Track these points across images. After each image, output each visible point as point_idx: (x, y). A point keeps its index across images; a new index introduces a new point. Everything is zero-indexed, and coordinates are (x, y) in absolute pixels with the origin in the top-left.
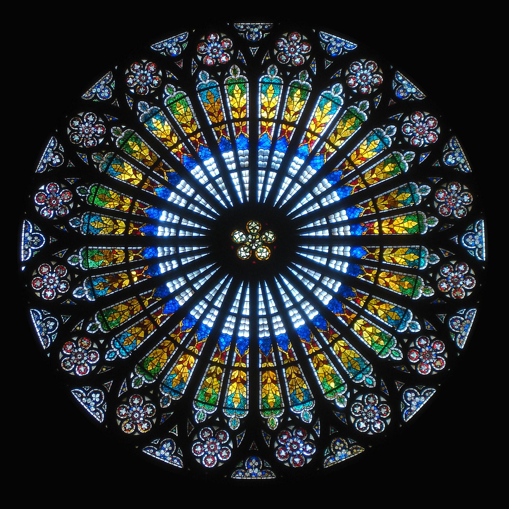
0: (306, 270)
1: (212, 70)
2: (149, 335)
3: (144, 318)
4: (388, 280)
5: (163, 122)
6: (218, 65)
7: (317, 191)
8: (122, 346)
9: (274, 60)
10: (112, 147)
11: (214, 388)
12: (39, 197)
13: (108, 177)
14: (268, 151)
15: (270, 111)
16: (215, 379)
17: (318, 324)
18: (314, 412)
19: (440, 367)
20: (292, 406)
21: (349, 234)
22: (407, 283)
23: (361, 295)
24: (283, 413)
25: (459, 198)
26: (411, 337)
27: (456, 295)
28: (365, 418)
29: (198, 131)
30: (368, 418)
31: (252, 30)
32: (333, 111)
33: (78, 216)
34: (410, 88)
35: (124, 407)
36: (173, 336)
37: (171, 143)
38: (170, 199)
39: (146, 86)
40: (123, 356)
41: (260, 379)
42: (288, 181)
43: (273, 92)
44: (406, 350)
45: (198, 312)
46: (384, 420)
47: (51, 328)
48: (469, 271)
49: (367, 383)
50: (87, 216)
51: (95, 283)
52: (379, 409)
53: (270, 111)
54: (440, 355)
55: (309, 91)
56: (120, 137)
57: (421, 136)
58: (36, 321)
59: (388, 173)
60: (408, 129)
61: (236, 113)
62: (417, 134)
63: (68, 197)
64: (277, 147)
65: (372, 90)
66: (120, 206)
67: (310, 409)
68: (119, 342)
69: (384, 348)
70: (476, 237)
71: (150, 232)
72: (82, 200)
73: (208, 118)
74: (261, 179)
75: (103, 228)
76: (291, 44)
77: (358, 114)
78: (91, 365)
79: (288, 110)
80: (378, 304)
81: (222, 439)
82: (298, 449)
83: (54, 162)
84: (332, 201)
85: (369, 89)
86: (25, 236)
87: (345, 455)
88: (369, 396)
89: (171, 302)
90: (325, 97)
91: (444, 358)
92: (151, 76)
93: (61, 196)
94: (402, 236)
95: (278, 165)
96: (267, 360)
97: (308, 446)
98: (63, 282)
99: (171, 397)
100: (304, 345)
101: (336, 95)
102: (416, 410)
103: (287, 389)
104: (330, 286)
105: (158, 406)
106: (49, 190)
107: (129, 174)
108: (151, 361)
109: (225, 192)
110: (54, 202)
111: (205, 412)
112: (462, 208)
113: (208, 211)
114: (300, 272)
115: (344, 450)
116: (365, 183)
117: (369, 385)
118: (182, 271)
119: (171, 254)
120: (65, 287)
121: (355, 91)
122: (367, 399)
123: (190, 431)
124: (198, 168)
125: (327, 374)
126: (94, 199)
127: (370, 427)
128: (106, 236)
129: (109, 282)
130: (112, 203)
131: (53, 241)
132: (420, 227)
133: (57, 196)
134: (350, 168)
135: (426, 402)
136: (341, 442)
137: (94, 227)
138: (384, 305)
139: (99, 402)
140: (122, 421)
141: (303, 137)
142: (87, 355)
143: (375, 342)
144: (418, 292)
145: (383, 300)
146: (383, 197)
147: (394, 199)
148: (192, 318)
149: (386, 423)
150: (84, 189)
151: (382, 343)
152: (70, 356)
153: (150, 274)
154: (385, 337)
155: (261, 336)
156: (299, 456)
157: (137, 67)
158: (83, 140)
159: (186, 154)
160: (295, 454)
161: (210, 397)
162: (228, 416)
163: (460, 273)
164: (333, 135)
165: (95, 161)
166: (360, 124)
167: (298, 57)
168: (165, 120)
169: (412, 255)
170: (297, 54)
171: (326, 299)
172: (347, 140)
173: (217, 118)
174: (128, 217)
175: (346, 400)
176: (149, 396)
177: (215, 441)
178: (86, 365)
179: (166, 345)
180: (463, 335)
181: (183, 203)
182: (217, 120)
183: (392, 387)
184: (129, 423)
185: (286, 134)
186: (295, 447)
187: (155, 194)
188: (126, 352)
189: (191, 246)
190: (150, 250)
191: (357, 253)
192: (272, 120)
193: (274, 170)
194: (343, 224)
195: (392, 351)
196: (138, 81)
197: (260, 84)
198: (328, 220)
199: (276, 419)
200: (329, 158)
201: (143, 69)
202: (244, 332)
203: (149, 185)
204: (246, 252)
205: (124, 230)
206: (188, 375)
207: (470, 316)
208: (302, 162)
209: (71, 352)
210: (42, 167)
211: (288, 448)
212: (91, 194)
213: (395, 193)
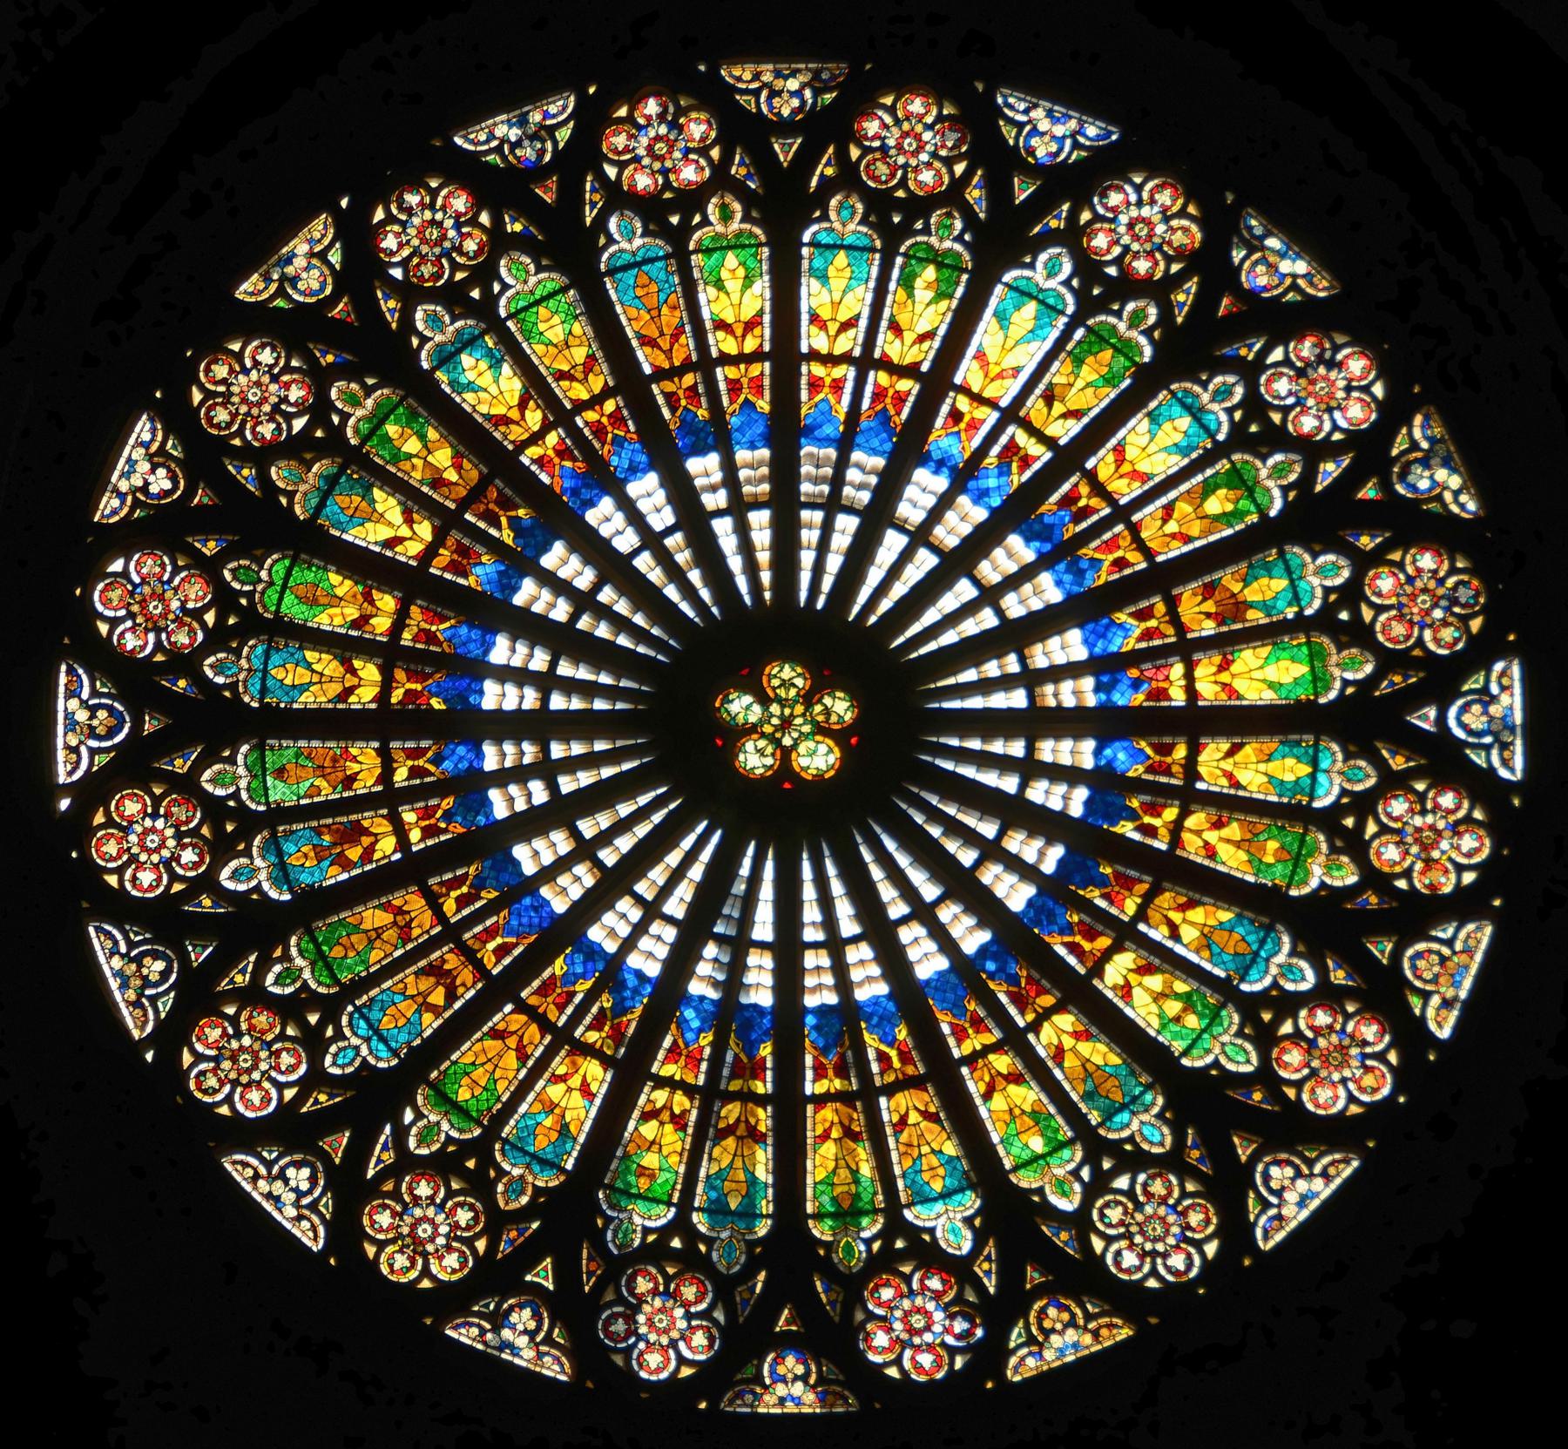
1: (650, 209)
2: (457, 998)
3: (445, 949)
4: (1212, 836)
5: (496, 365)
6: (668, 195)
7: (991, 570)
8: (377, 1032)
9: (848, 178)
10: (335, 444)
11: (665, 1152)
12: (110, 594)
13: (322, 532)
14: (832, 453)
16: (669, 1128)
17: (991, 966)
18: (977, 1222)
19: (1375, 1090)
20: (909, 1205)
21: (1091, 701)
23: (1128, 884)
26: (1287, 1004)
27: (1427, 882)
28: (1138, 1239)
29: (607, 393)
30: (1147, 1239)
31: (779, 84)
32: (1039, 332)
33: (229, 650)
35: (385, 1207)
36: (533, 1001)
37: (520, 430)
38: (519, 600)
39: (439, 258)
42: (892, 543)
43: (847, 273)
44: (1265, 1039)
45: (612, 933)
46: (1198, 1245)
47: (154, 977)
49: (1145, 1139)
50: (260, 650)
51: (289, 847)
52: (1184, 1214)
54: (1374, 1056)
55: (965, 270)
56: (360, 413)
57: (1323, 406)
59: (1216, 518)
60: (1282, 386)
61: (730, 339)
62: (1311, 402)
64: (859, 439)
66: (361, 622)
68: (367, 1020)
69: (1199, 1037)
72: (244, 602)
73: (640, 354)
74: (810, 536)
75: (311, 683)
76: (906, 126)
77: (1120, 338)
78: (281, 1086)
79: (896, 328)
80: (1182, 908)
81: (691, 1298)
82: (928, 1328)
83: (154, 489)
84: (1036, 605)
85: (1156, 263)
87: (1076, 1346)
88: (1152, 1177)
89: (527, 901)
90: (1016, 289)
92: (458, 226)
94: (1254, 710)
95: (865, 497)
96: (830, 1073)
98: (191, 844)
99: (530, 1179)
100: (946, 1029)
101: (1052, 284)
102: (1296, 1216)
103: (894, 1156)
104: (1030, 855)
106: (138, 572)
107: (390, 524)
108: (467, 1074)
109: (695, 576)
110: (155, 608)
113: (639, 634)
114: (936, 815)
115: (1070, 1332)
117: (1151, 1143)
118: (561, 812)
119: (527, 760)
120: (196, 859)
121: (1112, 271)
122: (1145, 1185)
124: (606, 504)
125: (1017, 1112)
126: (280, 600)
127: (1154, 1264)
128: (319, 711)
129: (334, 844)
130: (337, 611)
132: (1319, 679)
134: (1094, 502)
136: (1062, 1308)
139: (310, 1192)
140: (381, 1245)
141: (945, 409)
143: (1171, 1020)
144: (1308, 873)
145: (1197, 896)
147: (1234, 595)
148: (594, 951)
150: (248, 568)
151: (1192, 1021)
152: (216, 1060)
153: (459, 819)
154: (1205, 1006)
155: (811, 1001)
156: (930, 1348)
158: (244, 423)
159: (568, 464)
160: (917, 1340)
161: (652, 1177)
164: (1041, 404)
165: (281, 484)
167: (929, 165)
168: (502, 360)
169: (1290, 762)
170: (924, 157)
171: (1016, 895)
172: (1085, 420)
173: (668, 354)
174: (389, 654)
175: (1077, 1187)
176: (464, 1174)
177: (670, 1304)
178: (266, 1085)
179: (513, 1028)
181: (561, 611)
182: (670, 359)
183: (1220, 1152)
184: (401, 1251)
185: (888, 400)
186: (918, 1321)
187: (473, 585)
188: (390, 1048)
189: (589, 738)
190: (461, 750)
191: (1115, 758)
192: (846, 358)
193: (850, 510)
194: (1072, 670)
195: (1223, 1044)
196: (416, 242)
197: (805, 251)
198: (1022, 660)
201: (432, 206)
203: (455, 557)
204: (763, 755)
205: (377, 689)
206: (582, 1114)
207: (1472, 942)
208: (941, 483)
209: (219, 1049)
211: (898, 1326)
212: (271, 584)
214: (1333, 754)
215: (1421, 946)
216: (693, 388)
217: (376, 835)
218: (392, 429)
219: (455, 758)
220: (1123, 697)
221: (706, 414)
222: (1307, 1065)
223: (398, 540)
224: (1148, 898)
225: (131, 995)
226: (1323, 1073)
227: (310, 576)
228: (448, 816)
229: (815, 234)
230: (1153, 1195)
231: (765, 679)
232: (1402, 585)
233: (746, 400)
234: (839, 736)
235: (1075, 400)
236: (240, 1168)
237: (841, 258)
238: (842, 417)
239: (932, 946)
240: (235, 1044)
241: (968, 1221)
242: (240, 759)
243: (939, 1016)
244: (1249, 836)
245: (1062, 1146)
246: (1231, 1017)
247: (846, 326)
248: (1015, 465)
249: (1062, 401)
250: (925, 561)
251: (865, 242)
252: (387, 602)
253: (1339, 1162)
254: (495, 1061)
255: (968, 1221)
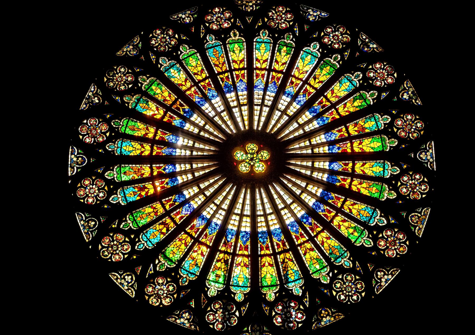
0: (294, 180)
3: (166, 218)
4: (359, 186)
7: (301, 121)
8: (149, 240)
9: (265, 26)
15: (263, 63)
17: (305, 220)
18: (303, 288)
19: (403, 252)
20: (286, 284)
21: (327, 152)
22: (374, 188)
23: (338, 199)
24: (278, 289)
25: (413, 124)
28: (345, 292)
29: (206, 78)
31: (247, 4)
34: (372, 45)
35: (151, 286)
36: (189, 231)
39: (165, 46)
40: (150, 247)
41: (260, 263)
42: (278, 113)
43: (265, 48)
44: (375, 239)
45: (209, 213)
46: (360, 293)
47: (92, 226)
48: (424, 179)
49: (345, 265)
50: (120, 142)
52: (356, 285)
53: (263, 63)
54: (402, 243)
56: (146, 83)
57: (382, 79)
58: (80, 221)
60: (372, 75)
61: (236, 64)
62: (379, 78)
63: (105, 128)
64: (269, 89)
65: (342, 46)
66: (146, 134)
67: (300, 286)
68: (146, 236)
69: (358, 238)
70: (427, 153)
71: (170, 153)
73: (214, 68)
74: (257, 113)
75: (133, 150)
78: (124, 254)
85: (340, 45)
86: (71, 157)
87: (329, 321)
88: (348, 275)
89: (187, 205)
90: (306, 52)
91: (406, 244)
92: (170, 38)
93: (99, 127)
96: (265, 249)
97: (299, 314)
99: (188, 278)
100: (294, 237)
101: (314, 50)
104: (314, 192)
105: (177, 283)
106: (90, 123)
107: (153, 110)
111: (216, 289)
112: (416, 132)
114: (290, 181)
116: (339, 114)
117: (347, 266)
120: (103, 195)
122: (346, 277)
123: (204, 303)
124: (207, 105)
125: (312, 258)
130: (140, 132)
131: (93, 160)
133: (96, 128)
135: (393, 278)
137: (125, 150)
138: (357, 205)
139: (131, 282)
141: (290, 81)
142: (121, 247)
145: (356, 202)
146: (354, 125)
147: (362, 126)
149: (361, 296)
150: (117, 122)
151: (356, 234)
152: (108, 247)
154: (359, 230)
157: (158, 32)
158: (117, 86)
159: (197, 95)
162: (234, 292)
163: (416, 181)
164: (313, 79)
165: (126, 101)
166: (333, 71)
167: (284, 23)
168: (180, 70)
171: (311, 202)
173: (221, 68)
175: (329, 278)
176: (171, 277)
178: (120, 254)
179: (184, 238)
180: (421, 227)
181: (196, 131)
184: (155, 298)
185: (275, 79)
188: (152, 244)
190: (170, 167)
192: (265, 69)
194: (323, 144)
195: (364, 240)
196: (159, 42)
197: (254, 43)
199: (273, 293)
200: (310, 96)
202: (246, 227)
203: (169, 118)
206: (201, 260)
207: (426, 213)
208: (289, 99)
210: (85, 106)
212: (123, 126)
213: (362, 121)
214: (389, 165)
215: (413, 214)
216: (228, 77)
217: (149, 189)
218: (153, 87)
219: (169, 169)
220: (335, 150)
221: (231, 83)
222: (386, 245)
223: (155, 115)
224: (344, 202)
225: (86, 231)
226: (390, 247)
227: (133, 124)
228: (167, 184)
229: (256, 39)
230: (348, 280)
231: (246, 148)
232: (403, 123)
233: (241, 79)
234: (266, 162)
235: (322, 79)
236: (114, 276)
237: (263, 45)
238: (264, 83)
239: (289, 215)
240: (112, 243)
241: (301, 287)
242: (115, 170)
243: (292, 233)
244: (368, 186)
245: (324, 267)
246: (366, 232)
247: (265, 61)
248: (307, 94)
249: (318, 79)
250: (286, 118)
251: (269, 41)
252: (152, 130)
253: (395, 270)
254: (179, 247)
255: (301, 287)
